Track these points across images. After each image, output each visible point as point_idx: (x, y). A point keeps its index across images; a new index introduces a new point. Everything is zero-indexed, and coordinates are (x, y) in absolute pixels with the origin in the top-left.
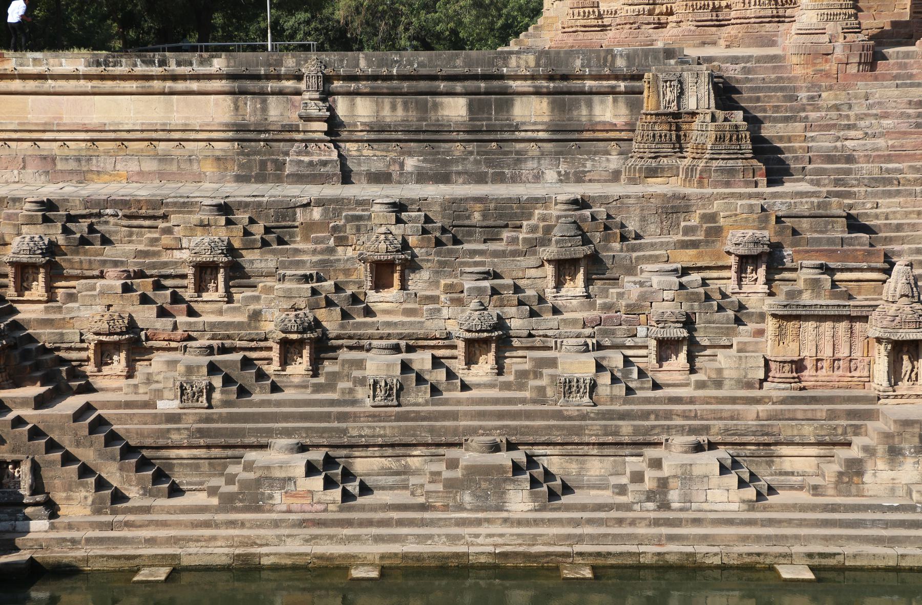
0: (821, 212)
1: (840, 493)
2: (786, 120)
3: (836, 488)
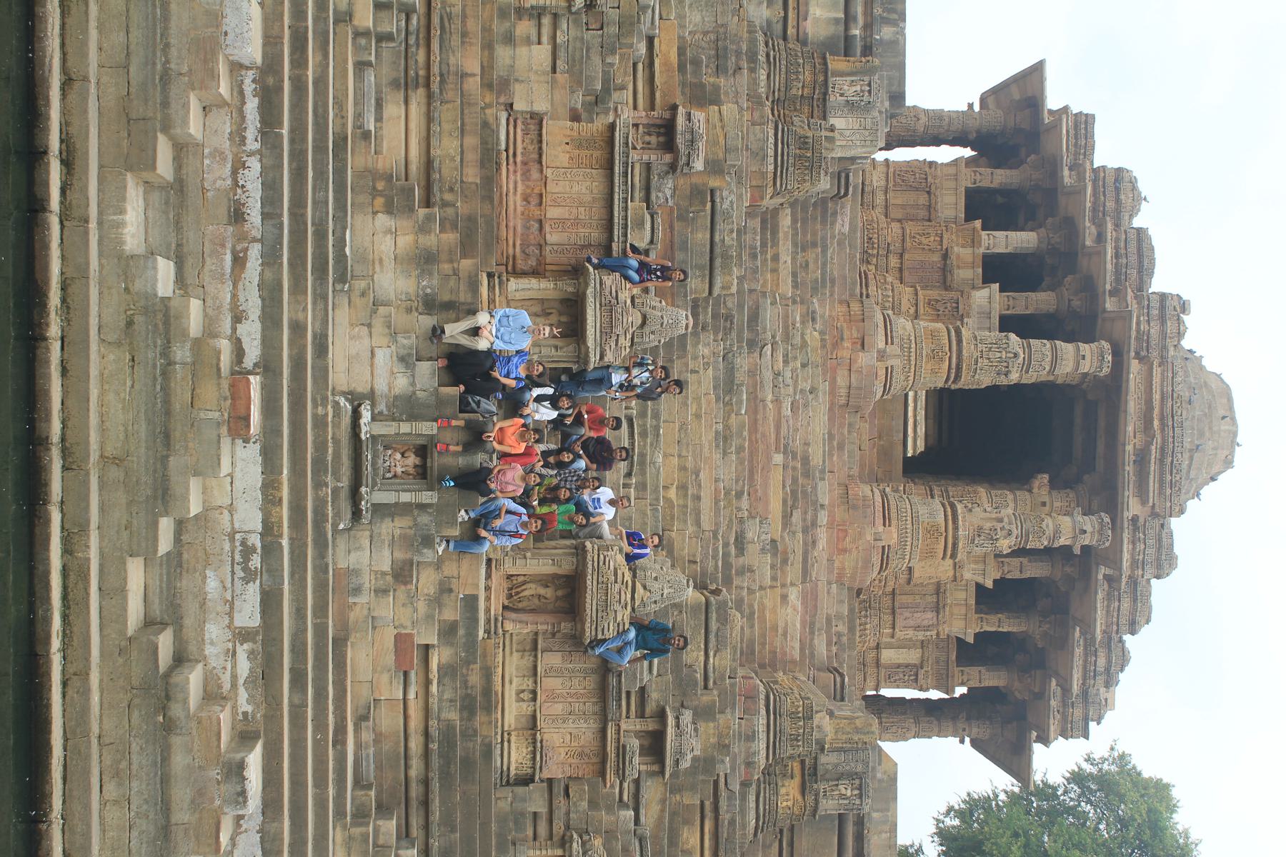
0: (718, 262)
1: (359, 175)
2: (794, 275)
3: (367, 170)
